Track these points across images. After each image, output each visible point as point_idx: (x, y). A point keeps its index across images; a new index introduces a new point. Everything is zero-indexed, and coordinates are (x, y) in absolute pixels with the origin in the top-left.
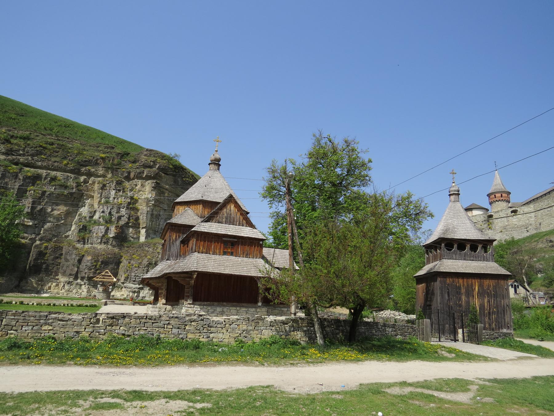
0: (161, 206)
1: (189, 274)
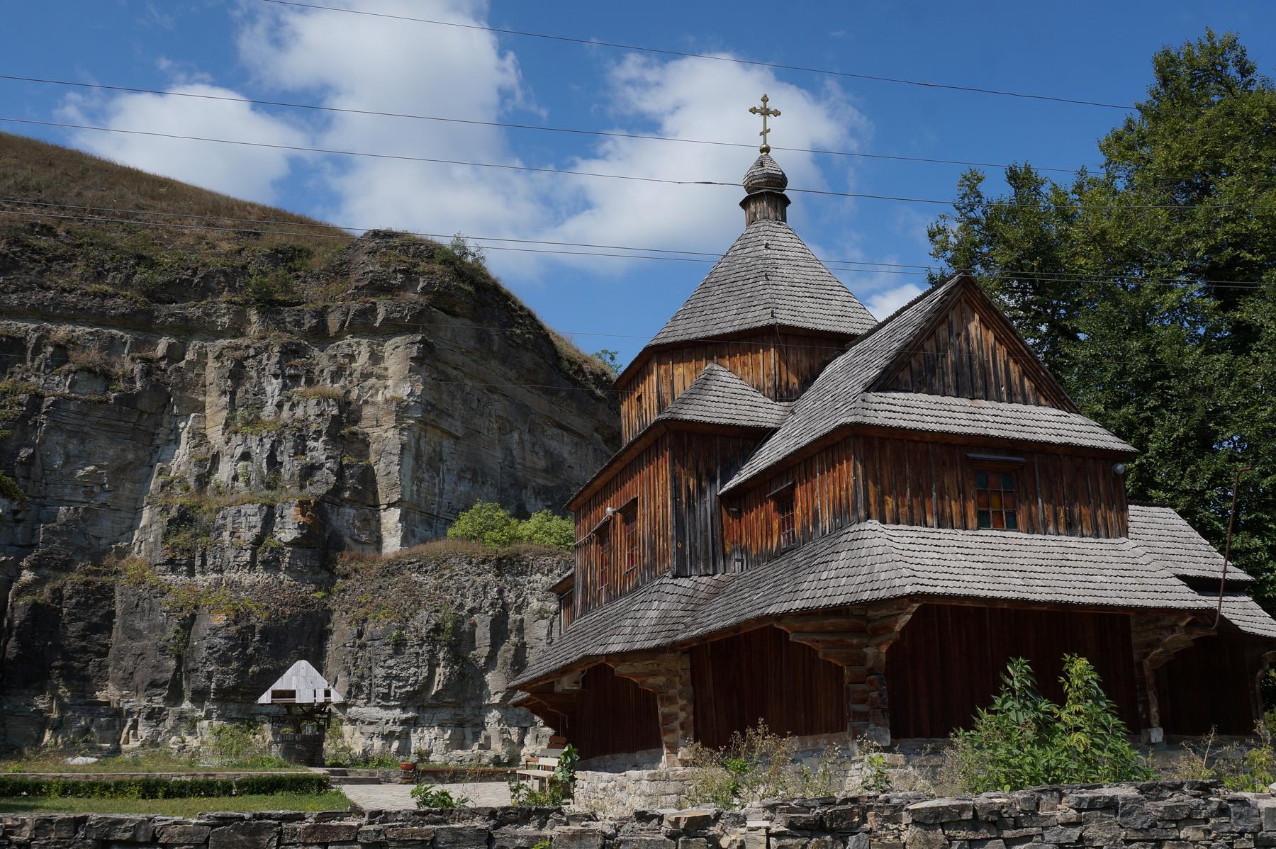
0: (445, 425)
1: (859, 618)
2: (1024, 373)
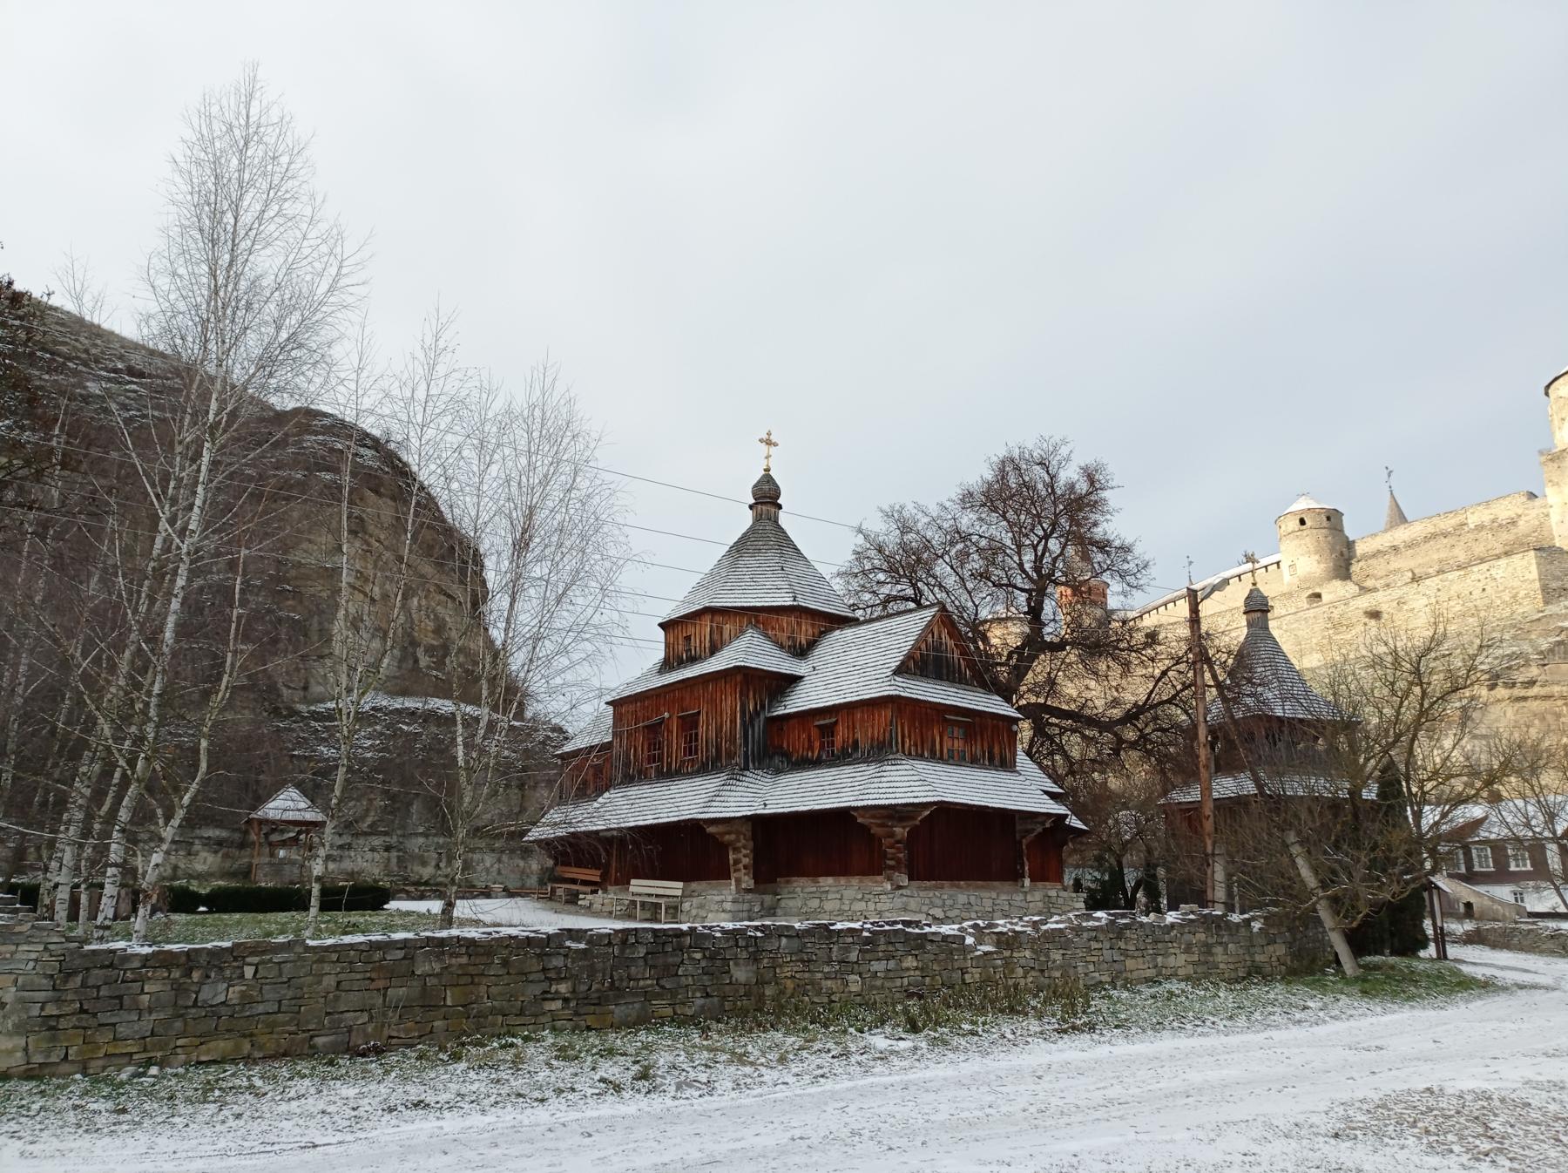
2: (967, 666)
